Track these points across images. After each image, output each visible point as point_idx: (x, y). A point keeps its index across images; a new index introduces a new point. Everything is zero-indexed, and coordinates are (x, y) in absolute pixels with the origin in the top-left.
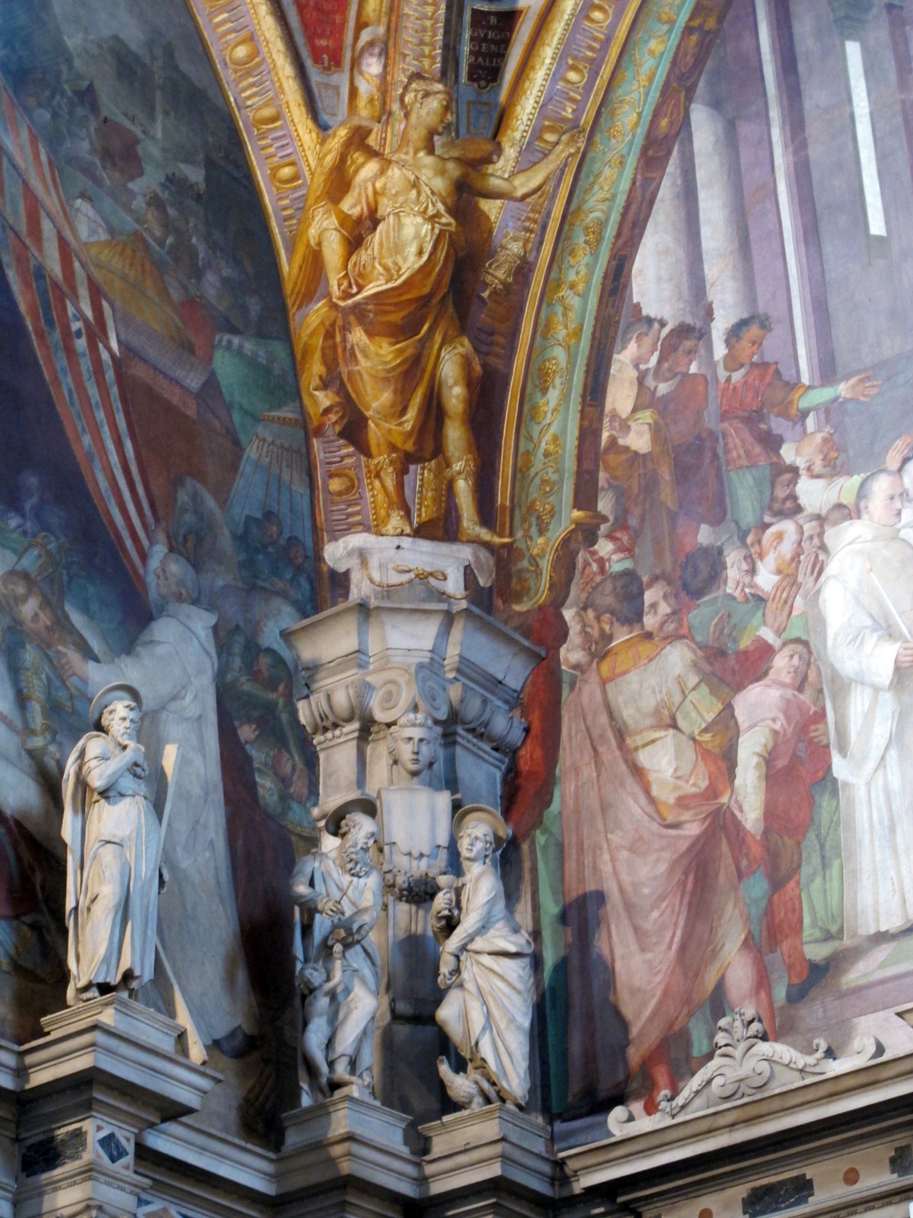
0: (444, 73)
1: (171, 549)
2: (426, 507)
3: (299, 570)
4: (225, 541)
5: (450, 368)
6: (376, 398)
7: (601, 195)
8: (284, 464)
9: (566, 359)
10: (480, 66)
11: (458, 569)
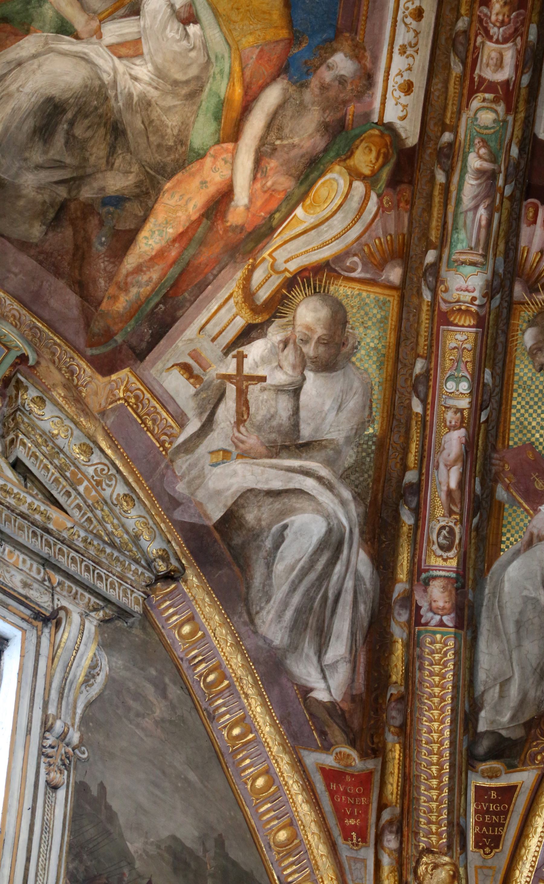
0: (450, 847)
10: (484, 835)
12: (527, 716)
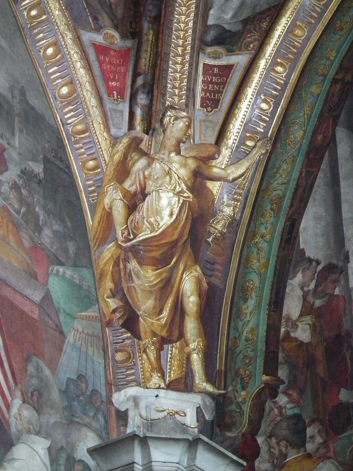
0: (187, 105)
1: (24, 401)
2: (174, 370)
3: (98, 409)
4: (55, 395)
5: (189, 284)
6: (145, 304)
7: (280, 181)
8: (89, 344)
9: (260, 282)
10: (207, 98)
11: (193, 409)
12: (244, 16)
